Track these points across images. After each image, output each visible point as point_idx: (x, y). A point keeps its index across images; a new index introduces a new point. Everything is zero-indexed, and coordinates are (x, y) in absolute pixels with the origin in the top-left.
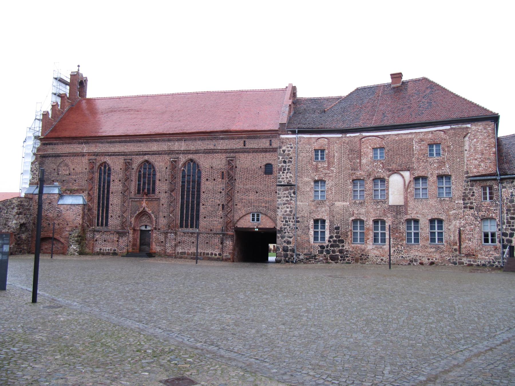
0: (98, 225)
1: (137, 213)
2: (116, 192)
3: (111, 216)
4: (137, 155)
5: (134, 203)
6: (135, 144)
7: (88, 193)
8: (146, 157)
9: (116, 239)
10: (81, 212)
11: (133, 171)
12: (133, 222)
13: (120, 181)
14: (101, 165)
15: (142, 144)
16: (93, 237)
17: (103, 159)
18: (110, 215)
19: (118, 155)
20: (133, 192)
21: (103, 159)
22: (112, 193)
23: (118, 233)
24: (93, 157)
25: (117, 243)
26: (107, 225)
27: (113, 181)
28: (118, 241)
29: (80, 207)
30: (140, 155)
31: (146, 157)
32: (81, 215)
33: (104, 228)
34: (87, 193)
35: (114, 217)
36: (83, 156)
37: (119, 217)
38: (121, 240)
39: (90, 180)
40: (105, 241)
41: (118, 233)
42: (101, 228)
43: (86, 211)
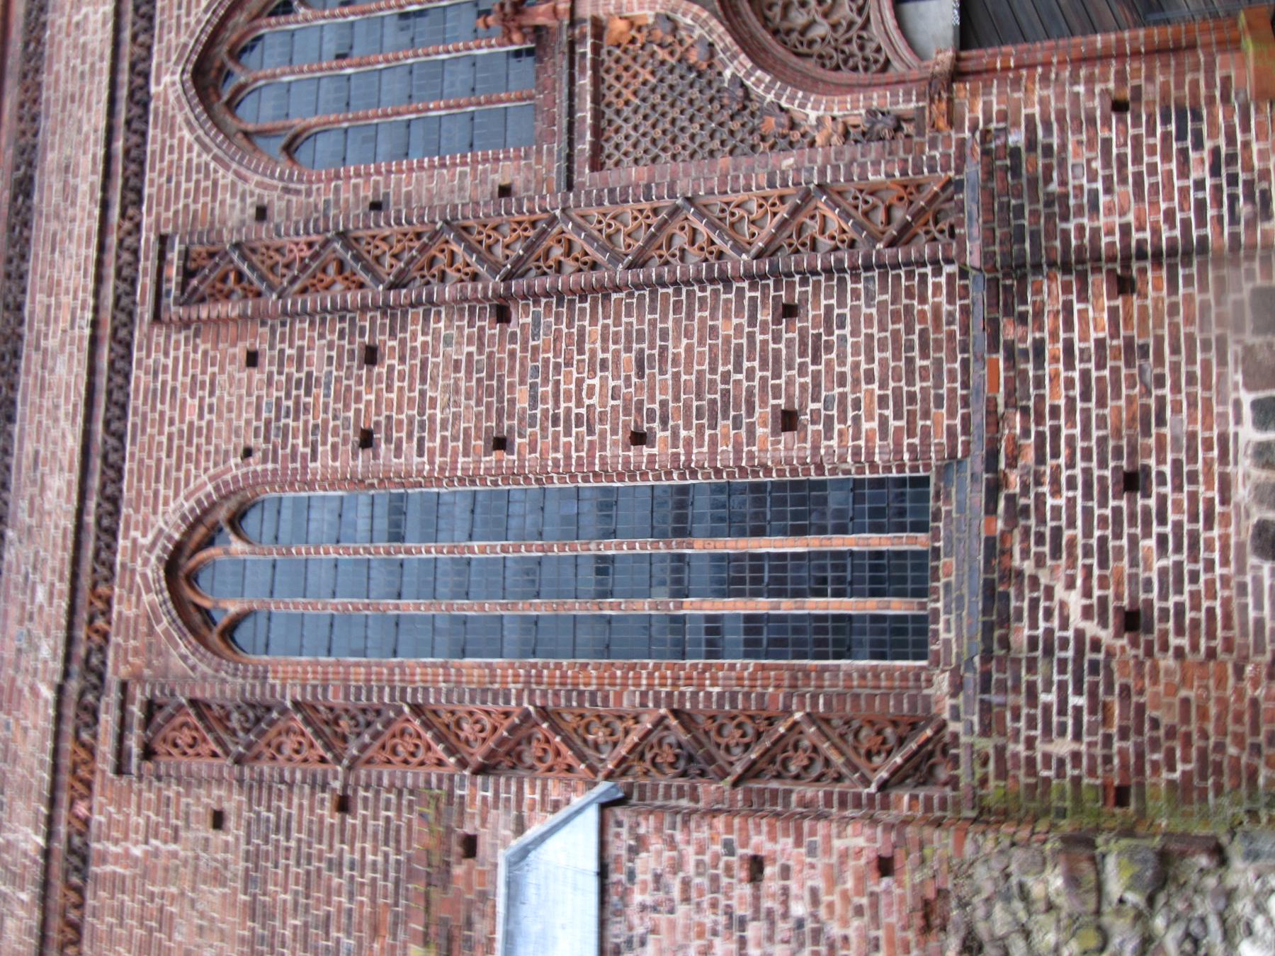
0: (907, 638)
1: (735, 66)
2: (491, 387)
3: (788, 420)
4: (134, 195)
5: (623, 134)
6: (42, 228)
7: (481, 770)
8: (168, 82)
9: (1097, 312)
10: (702, 844)
11: (277, 205)
12: (851, 108)
13: (371, 356)
14: (196, 622)
15: (52, 156)
16: (1088, 665)
17: (139, 596)
18: (777, 453)
19: (120, 407)
20: (506, 173)
21: (139, 596)
22: (501, 444)
23: (1008, 280)
24: (108, 720)
25: (1153, 284)
26: (897, 499)
27: (366, 440)
28: (1124, 286)
29: (646, 864)
30: (136, 158)
31: (168, 82)
32: (760, 842)
33: (955, 539)
34: (475, 792)
35: (794, 381)
36: (80, 857)
37: (789, 311)
38: (1109, 220)
39: (334, 741)
40: (1133, 482)
41: (1008, 280)
42: (948, 569)
43: (708, 790)
